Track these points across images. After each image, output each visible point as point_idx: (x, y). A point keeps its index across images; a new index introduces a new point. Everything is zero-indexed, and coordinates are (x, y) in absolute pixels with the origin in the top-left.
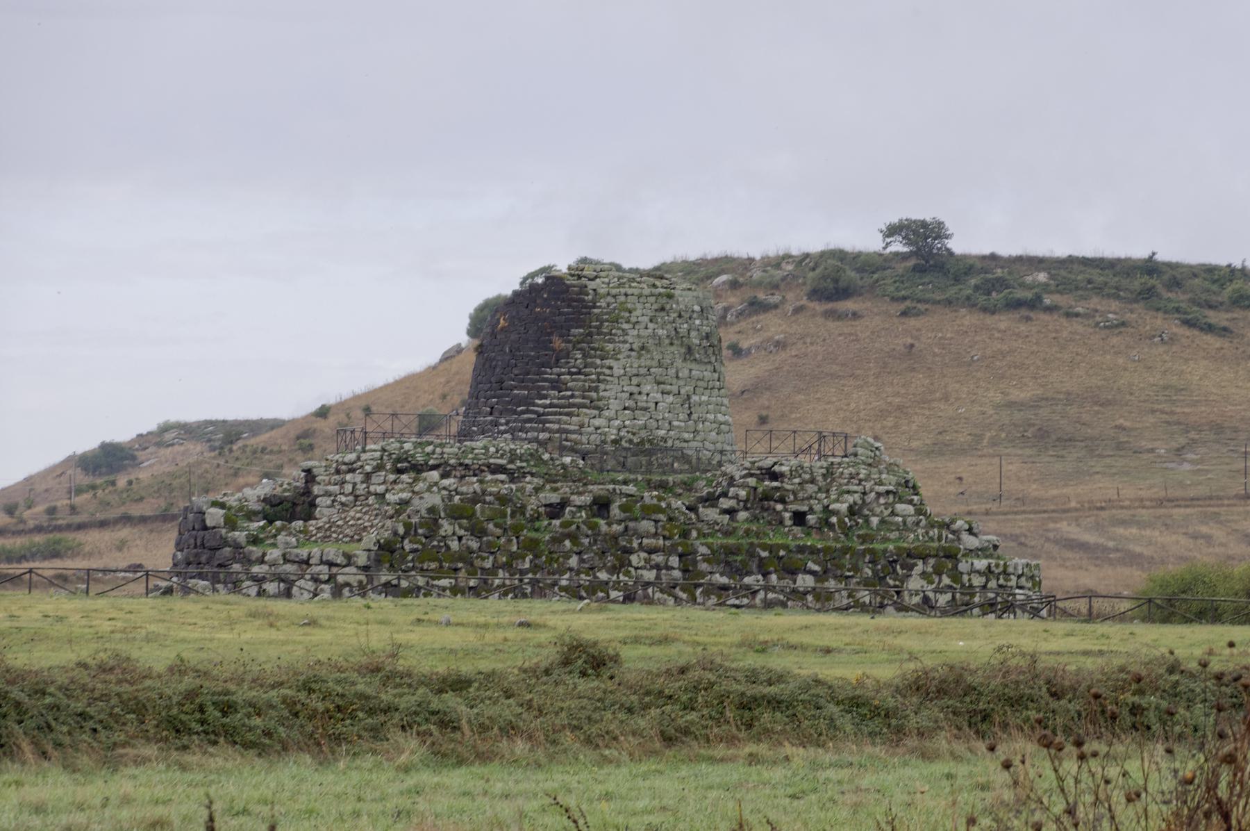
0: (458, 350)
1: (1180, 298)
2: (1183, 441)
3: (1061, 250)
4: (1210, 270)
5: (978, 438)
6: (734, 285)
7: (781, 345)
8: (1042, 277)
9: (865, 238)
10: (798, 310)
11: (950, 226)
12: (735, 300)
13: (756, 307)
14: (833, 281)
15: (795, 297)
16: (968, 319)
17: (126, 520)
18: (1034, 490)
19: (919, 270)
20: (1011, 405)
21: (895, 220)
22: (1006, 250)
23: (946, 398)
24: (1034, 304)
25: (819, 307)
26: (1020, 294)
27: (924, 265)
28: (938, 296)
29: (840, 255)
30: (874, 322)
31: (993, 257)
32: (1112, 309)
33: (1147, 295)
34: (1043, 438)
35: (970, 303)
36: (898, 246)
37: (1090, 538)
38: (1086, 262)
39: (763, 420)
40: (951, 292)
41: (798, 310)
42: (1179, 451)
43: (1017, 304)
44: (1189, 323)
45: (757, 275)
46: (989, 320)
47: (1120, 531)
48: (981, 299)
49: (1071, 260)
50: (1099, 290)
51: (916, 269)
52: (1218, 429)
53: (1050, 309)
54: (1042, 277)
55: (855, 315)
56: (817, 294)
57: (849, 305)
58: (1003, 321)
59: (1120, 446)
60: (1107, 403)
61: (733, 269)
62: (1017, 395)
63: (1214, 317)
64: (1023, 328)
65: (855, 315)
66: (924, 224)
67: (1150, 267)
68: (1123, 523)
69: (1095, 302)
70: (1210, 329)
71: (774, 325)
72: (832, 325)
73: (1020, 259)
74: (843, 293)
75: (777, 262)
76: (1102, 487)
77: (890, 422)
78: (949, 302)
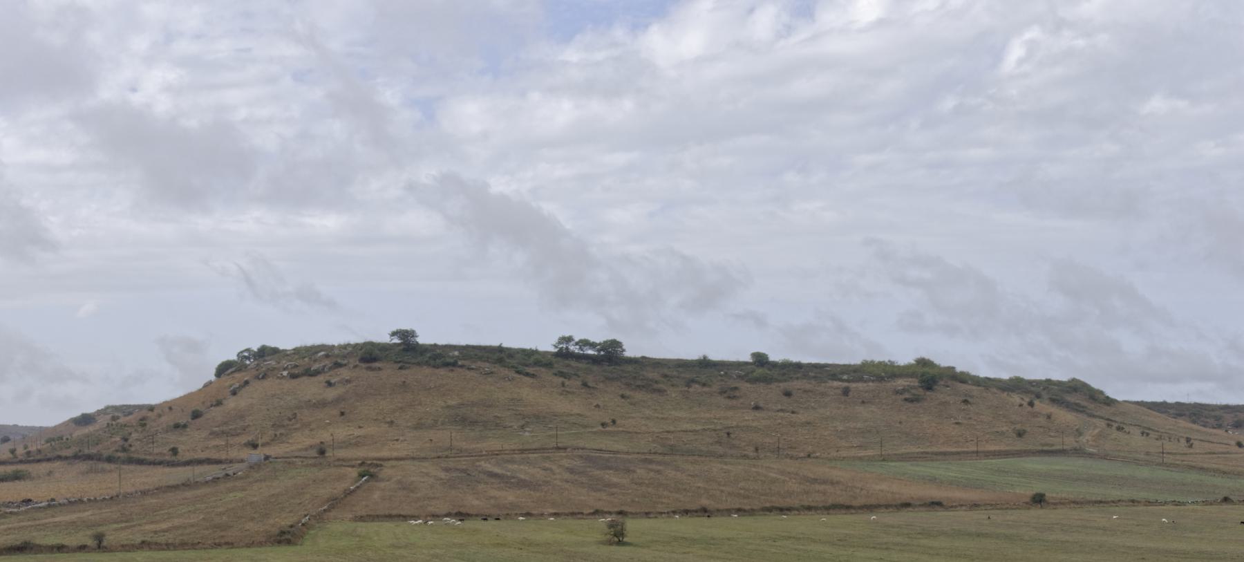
0: (211, 383)
1: (513, 362)
2: (523, 422)
3: (463, 343)
4: (523, 351)
5: (436, 422)
6: (327, 356)
7: (348, 381)
8: (456, 353)
9: (382, 335)
10: (355, 367)
11: (418, 332)
12: (328, 362)
13: (338, 365)
14: (369, 354)
15: (353, 361)
16: (427, 370)
17: (59, 458)
18: (464, 445)
19: (405, 350)
20: (448, 407)
21: (395, 329)
22: (441, 342)
23: (420, 404)
24: (454, 364)
25: (364, 365)
26: (448, 360)
27: (407, 349)
28: (413, 361)
29: (372, 344)
30: (388, 373)
31: (435, 345)
32: (487, 367)
33: (500, 361)
34: (463, 421)
35: (427, 364)
36: (396, 340)
37: (497, 470)
38: (474, 347)
39: (342, 414)
40: (420, 359)
41: (355, 367)
42: (522, 427)
43: (447, 365)
44: (518, 372)
45: (336, 352)
46: (437, 371)
47: (510, 466)
48: (432, 362)
49: (467, 347)
50: (481, 358)
51: (404, 350)
52: (537, 417)
53: (462, 366)
54: (456, 353)
55: (380, 369)
56: (363, 360)
57: (377, 365)
58: (442, 371)
59: (497, 425)
60: (490, 406)
61: (327, 350)
62: (451, 403)
63: (530, 370)
64: (451, 374)
65: (380, 369)
66: (407, 331)
67: (500, 349)
68: (508, 461)
69: (479, 364)
70: (527, 374)
71: (345, 373)
72: (371, 374)
73: (446, 346)
74: (375, 360)
75: (345, 347)
76: (494, 444)
77: (397, 414)
78: (419, 364)
